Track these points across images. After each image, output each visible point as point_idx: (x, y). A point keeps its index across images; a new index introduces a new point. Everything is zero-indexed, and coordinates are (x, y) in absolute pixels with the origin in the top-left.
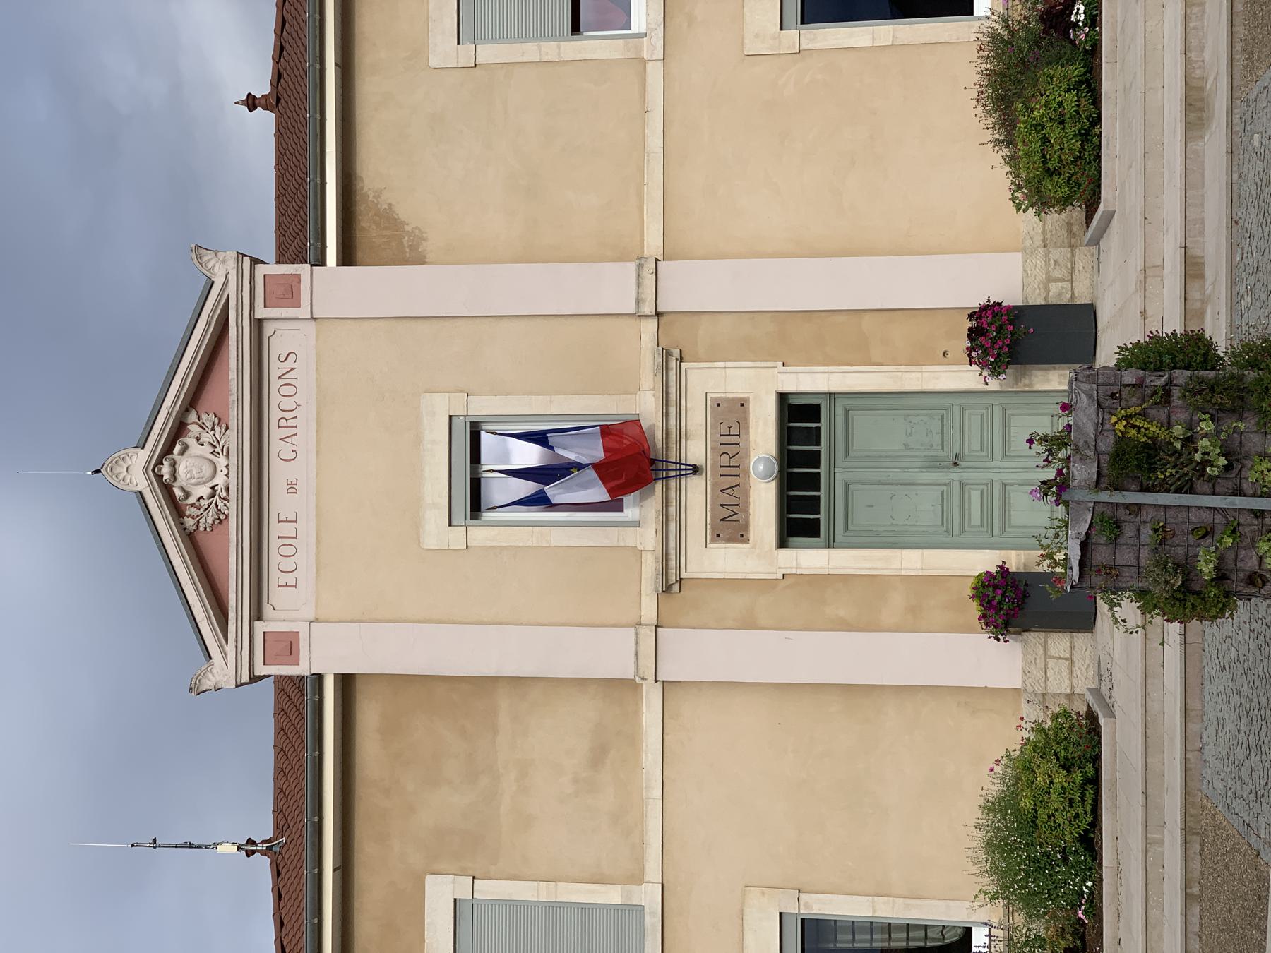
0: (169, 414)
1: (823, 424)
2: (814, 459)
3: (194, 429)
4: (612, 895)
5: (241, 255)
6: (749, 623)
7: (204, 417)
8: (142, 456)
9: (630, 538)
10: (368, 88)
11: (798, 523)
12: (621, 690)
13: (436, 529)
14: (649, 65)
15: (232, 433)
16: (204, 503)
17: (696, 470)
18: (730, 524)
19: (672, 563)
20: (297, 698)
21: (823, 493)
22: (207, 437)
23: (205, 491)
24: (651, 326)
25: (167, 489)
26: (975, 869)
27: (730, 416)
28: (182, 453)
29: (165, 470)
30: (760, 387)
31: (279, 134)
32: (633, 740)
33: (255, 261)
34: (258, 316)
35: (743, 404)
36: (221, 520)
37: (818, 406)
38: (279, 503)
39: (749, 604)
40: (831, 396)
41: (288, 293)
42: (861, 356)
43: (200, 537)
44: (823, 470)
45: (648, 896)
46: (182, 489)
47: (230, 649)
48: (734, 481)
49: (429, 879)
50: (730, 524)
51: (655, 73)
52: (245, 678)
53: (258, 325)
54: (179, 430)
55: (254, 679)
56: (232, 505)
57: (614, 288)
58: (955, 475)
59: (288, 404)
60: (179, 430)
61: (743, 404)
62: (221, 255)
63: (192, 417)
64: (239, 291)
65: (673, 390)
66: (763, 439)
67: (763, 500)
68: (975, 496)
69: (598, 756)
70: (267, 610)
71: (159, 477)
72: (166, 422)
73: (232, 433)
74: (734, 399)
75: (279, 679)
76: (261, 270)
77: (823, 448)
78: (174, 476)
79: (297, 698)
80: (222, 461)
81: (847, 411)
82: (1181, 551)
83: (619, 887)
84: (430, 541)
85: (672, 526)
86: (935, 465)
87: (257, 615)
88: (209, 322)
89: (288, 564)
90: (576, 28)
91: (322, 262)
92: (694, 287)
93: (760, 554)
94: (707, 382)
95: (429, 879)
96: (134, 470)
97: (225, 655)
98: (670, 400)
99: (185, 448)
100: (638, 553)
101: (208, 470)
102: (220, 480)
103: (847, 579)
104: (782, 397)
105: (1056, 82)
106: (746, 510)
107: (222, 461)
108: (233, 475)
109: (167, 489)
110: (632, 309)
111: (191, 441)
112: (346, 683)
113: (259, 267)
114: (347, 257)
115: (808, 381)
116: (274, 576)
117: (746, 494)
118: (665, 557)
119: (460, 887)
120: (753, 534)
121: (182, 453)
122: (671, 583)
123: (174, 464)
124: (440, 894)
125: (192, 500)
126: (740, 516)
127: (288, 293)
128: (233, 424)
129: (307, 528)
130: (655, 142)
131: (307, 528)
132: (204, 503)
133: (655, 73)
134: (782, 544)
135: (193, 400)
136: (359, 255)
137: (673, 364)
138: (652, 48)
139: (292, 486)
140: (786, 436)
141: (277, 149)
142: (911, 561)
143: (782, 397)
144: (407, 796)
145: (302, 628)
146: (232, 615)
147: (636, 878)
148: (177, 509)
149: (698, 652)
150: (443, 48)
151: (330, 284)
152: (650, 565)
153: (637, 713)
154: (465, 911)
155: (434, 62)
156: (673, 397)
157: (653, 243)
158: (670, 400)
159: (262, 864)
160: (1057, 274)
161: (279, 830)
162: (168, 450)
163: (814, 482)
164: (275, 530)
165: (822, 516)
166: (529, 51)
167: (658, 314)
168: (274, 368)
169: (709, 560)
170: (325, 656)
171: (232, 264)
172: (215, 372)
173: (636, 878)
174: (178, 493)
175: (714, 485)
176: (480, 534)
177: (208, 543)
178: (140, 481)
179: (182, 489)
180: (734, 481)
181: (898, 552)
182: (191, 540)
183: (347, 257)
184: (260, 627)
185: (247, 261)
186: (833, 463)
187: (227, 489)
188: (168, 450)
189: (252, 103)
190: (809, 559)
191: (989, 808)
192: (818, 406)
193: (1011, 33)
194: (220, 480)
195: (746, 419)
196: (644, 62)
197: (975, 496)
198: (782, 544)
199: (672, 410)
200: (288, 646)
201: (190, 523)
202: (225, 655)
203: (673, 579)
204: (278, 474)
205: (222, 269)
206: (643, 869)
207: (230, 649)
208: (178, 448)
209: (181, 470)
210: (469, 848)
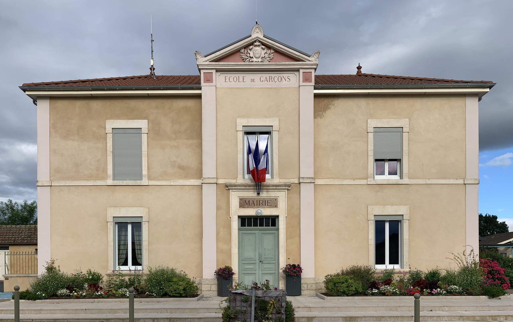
0: (273, 44)
1: (271, 227)
2: (262, 225)
3: (269, 52)
4: (145, 172)
5: (317, 65)
6: (218, 208)
7: (272, 55)
8: (261, 36)
9: (240, 176)
10: (362, 102)
11: (245, 221)
12: (199, 174)
13: (242, 122)
14: (366, 180)
15: (268, 63)
16: (248, 55)
17: (258, 194)
18: (244, 203)
19: (234, 188)
20: (194, 82)
21: (252, 227)
22: (266, 55)
23: (251, 55)
24: (296, 181)
25: (252, 44)
26: (157, 267)
28: (262, 48)
29: (257, 43)
30: (280, 211)
31: (350, 76)
33: (315, 69)
34: (300, 70)
35: (276, 206)
36: (243, 60)
37: (275, 226)
38: (248, 77)
39: (223, 208)
40: (278, 229)
41: (307, 79)
43: (238, 54)
44: (259, 227)
45: (145, 181)
46: (252, 48)
47: (208, 63)
48: (256, 204)
49: (146, 121)
51: (364, 182)
52: (200, 67)
53: (298, 70)
54: (269, 47)
55: (200, 70)
56: (248, 63)
57: (307, 171)
58: (257, 261)
59: (276, 79)
60: (269, 47)
61: (276, 206)
62: (317, 59)
63: (272, 51)
64: (307, 65)
65: (280, 188)
67: (251, 212)
68: (252, 267)
69: (181, 168)
70: (219, 74)
71: (255, 41)
72: (271, 43)
73: (268, 63)
75: (199, 77)
76: (313, 71)
77: (264, 227)
78: (256, 46)
79: (194, 82)
80: (260, 60)
81: (274, 233)
82: (240, 317)
83: (147, 173)
84: (238, 120)
85: (243, 187)
86: (260, 256)
87: (217, 71)
88: (298, 56)
89: (231, 79)
90: (376, 160)
91: (315, 89)
93: (236, 211)
94: (282, 196)
95: (146, 121)
96: (257, 34)
97: (206, 61)
98: (277, 187)
99: (264, 49)
100: (236, 178)
101: (257, 56)
102: (255, 59)
103: (230, 234)
104: (278, 217)
105: (358, 285)
107: (260, 60)
108: (256, 63)
109: (252, 44)
111: (265, 51)
112: (199, 96)
113: (314, 70)
115: (282, 223)
116: (229, 75)
117: (252, 208)
118: (235, 186)
119: (145, 130)
120: (242, 209)
121: (262, 48)
122: (228, 187)
123: (259, 46)
124: (143, 124)
125: (249, 51)
127: (307, 79)
128: (270, 63)
129: (241, 85)
131: (241, 85)
132: (248, 55)
134: (239, 217)
135: (277, 51)
136: (317, 99)
137: (287, 188)
138: (370, 181)
139: (253, 80)
140: (267, 218)
141: (346, 75)
142: (235, 250)
143: (278, 217)
144: (169, 113)
145: (214, 83)
146: (217, 63)
147: (149, 178)
148: (246, 47)
149: (210, 195)
150: (373, 123)
151: (309, 91)
152: (233, 181)
153: (193, 178)
154: (138, 131)
155: (369, 120)
156: (278, 188)
157: (319, 182)
158: (277, 187)
159: (148, 72)
160: (309, 286)
161: (158, 77)
162: (263, 44)
163: (255, 225)
164: (241, 75)
165: (246, 227)
166: (371, 147)
167: (300, 183)
168: (285, 75)
169: (235, 197)
170: (207, 91)
171: (315, 62)
172: (285, 57)
173: (149, 178)
174: (251, 47)
176: (240, 134)
177: (237, 56)
178: (254, 36)
179: (252, 48)
180: (256, 204)
181: (237, 247)
182: (237, 51)
183: (316, 96)
184: (214, 71)
185: (315, 67)
186: (260, 230)
187: (252, 62)
188: (263, 44)
189: (359, 68)
190: (235, 224)
191: (172, 270)
192: (275, 226)
193: (371, 274)
194: (255, 59)
195: (272, 207)
196: (367, 179)
197: (252, 267)
198: (239, 217)
199: (274, 188)
200: (209, 80)
201: (242, 51)
202: (206, 61)
203: (229, 188)
204: (257, 76)
205: (313, 60)
206: (152, 180)
207: (208, 63)
208: (264, 47)
209: (257, 48)
210: (156, 132)
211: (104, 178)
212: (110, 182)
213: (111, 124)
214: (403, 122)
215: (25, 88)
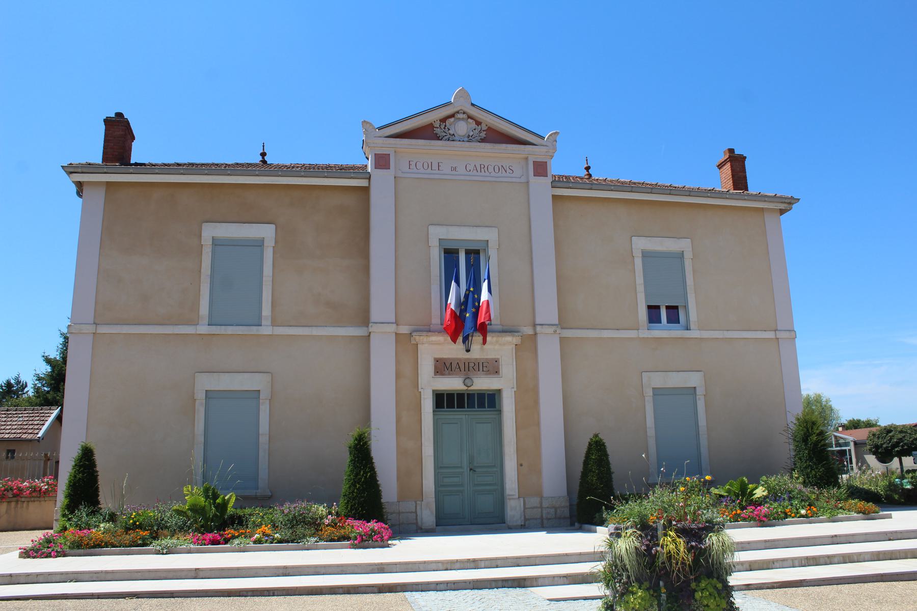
4: (266, 311)
6: (398, 376)
11: (443, 400)
13: (438, 233)
27: (492, 368)
29: (460, 116)
32: (338, 323)
40: (500, 412)
42: (519, 427)
45: (266, 330)
48: (462, 369)
50: (443, 367)
66: (482, 383)
67: (453, 384)
68: (456, 480)
74: (498, 368)
83: (270, 314)
86: (471, 459)
92: (549, 352)
95: (273, 226)
104: (499, 391)
106: (449, 374)
109: (452, 116)
110: (538, 321)
114: (555, 197)
123: (463, 119)
124: (266, 232)
126: (447, 372)
130: (606, 334)
133: (632, 334)
142: (428, 450)
143: (499, 391)
150: (641, 244)
173: (274, 324)
175: (460, 359)
180: (462, 369)
183: (555, 197)
188: (469, 117)
190: (428, 404)
197: (456, 480)
210: (287, 244)
211: (194, 322)
212: (203, 329)
213: (211, 231)
214: (684, 245)
215: (70, 170)
